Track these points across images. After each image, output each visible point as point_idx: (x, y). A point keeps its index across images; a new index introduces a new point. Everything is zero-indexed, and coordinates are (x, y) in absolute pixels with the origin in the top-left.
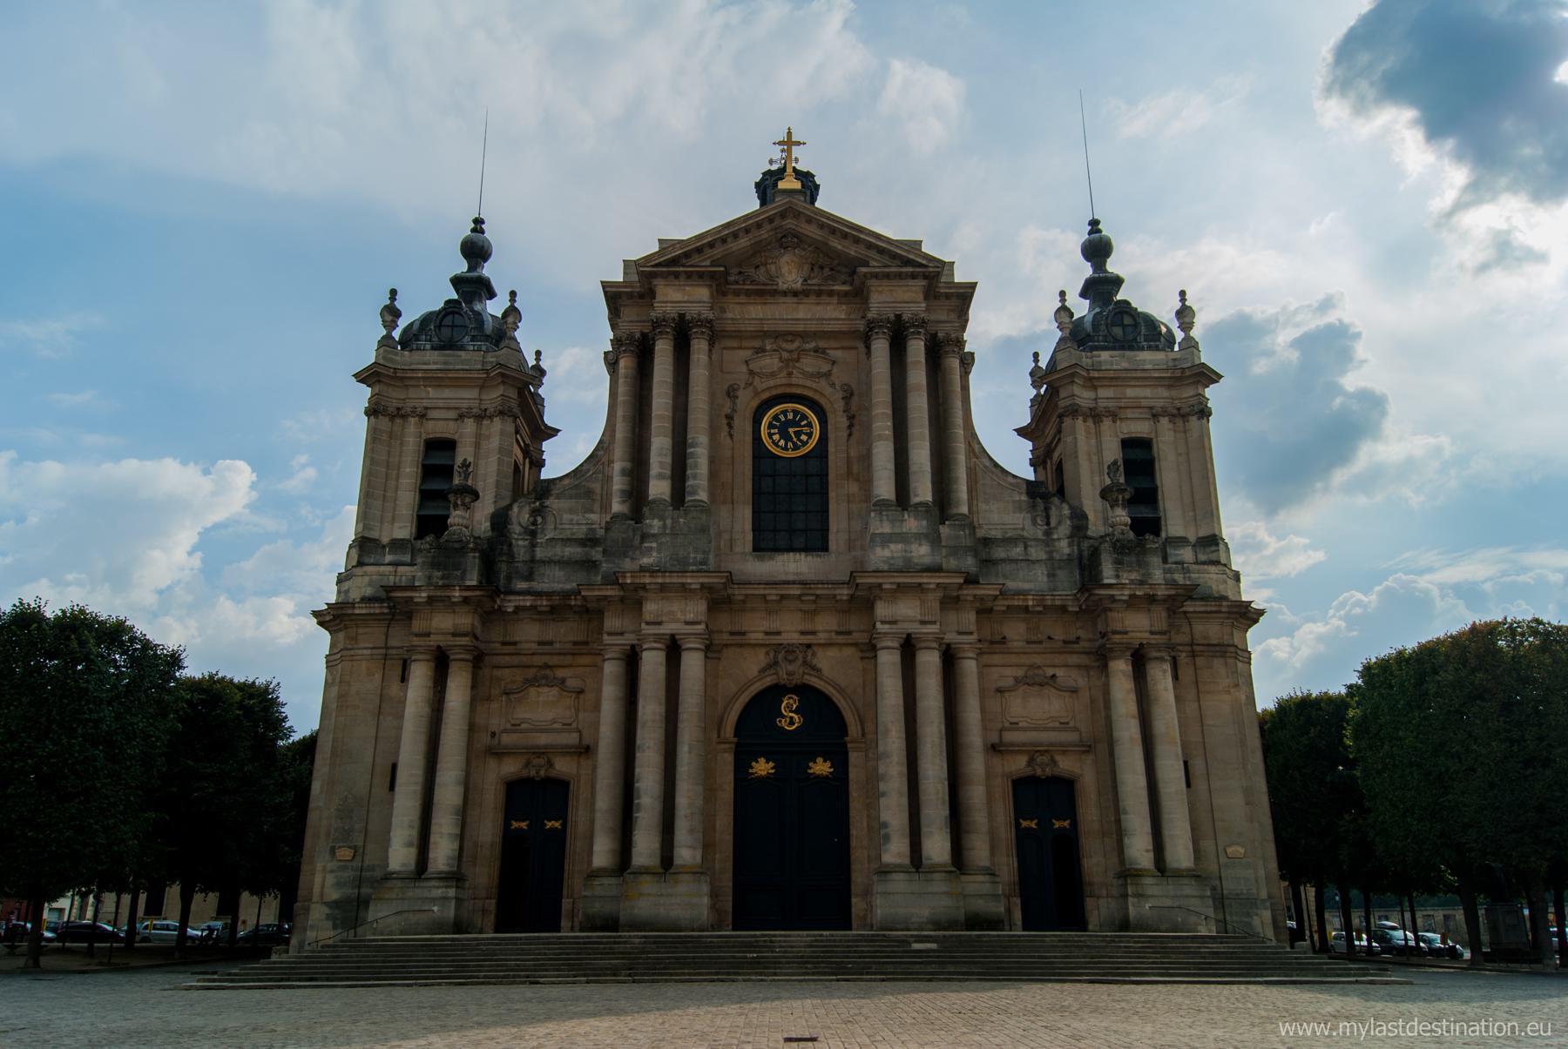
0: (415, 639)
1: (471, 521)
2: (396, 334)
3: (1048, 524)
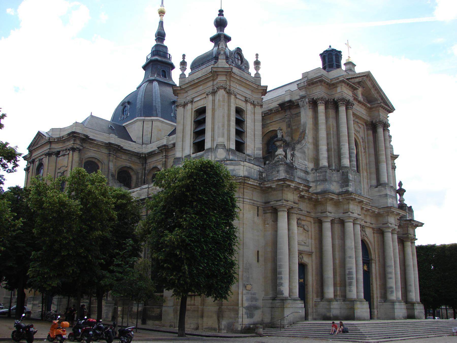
0: (284, 202)
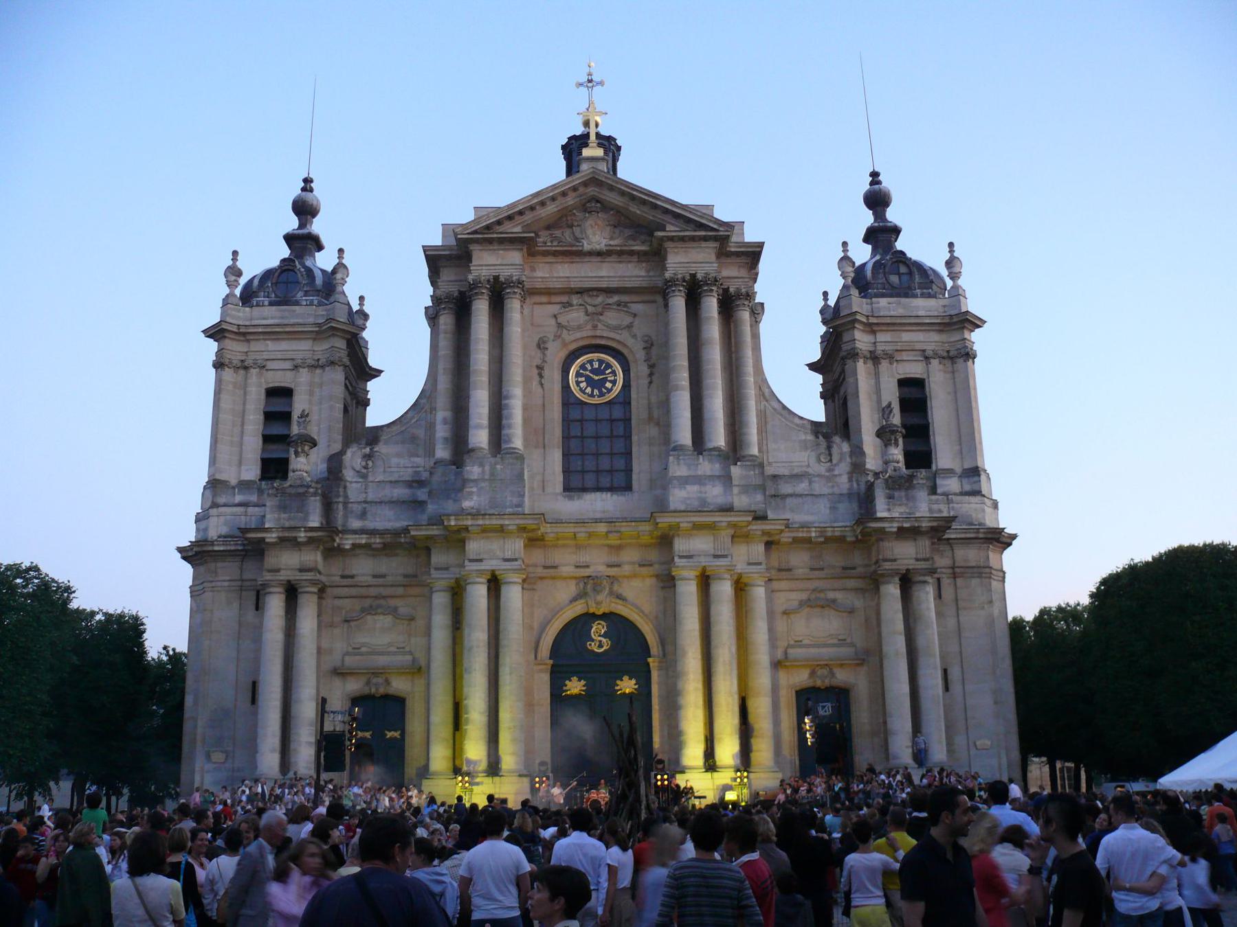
0: (268, 574)
1: (306, 465)
2: (238, 292)
3: (831, 460)
